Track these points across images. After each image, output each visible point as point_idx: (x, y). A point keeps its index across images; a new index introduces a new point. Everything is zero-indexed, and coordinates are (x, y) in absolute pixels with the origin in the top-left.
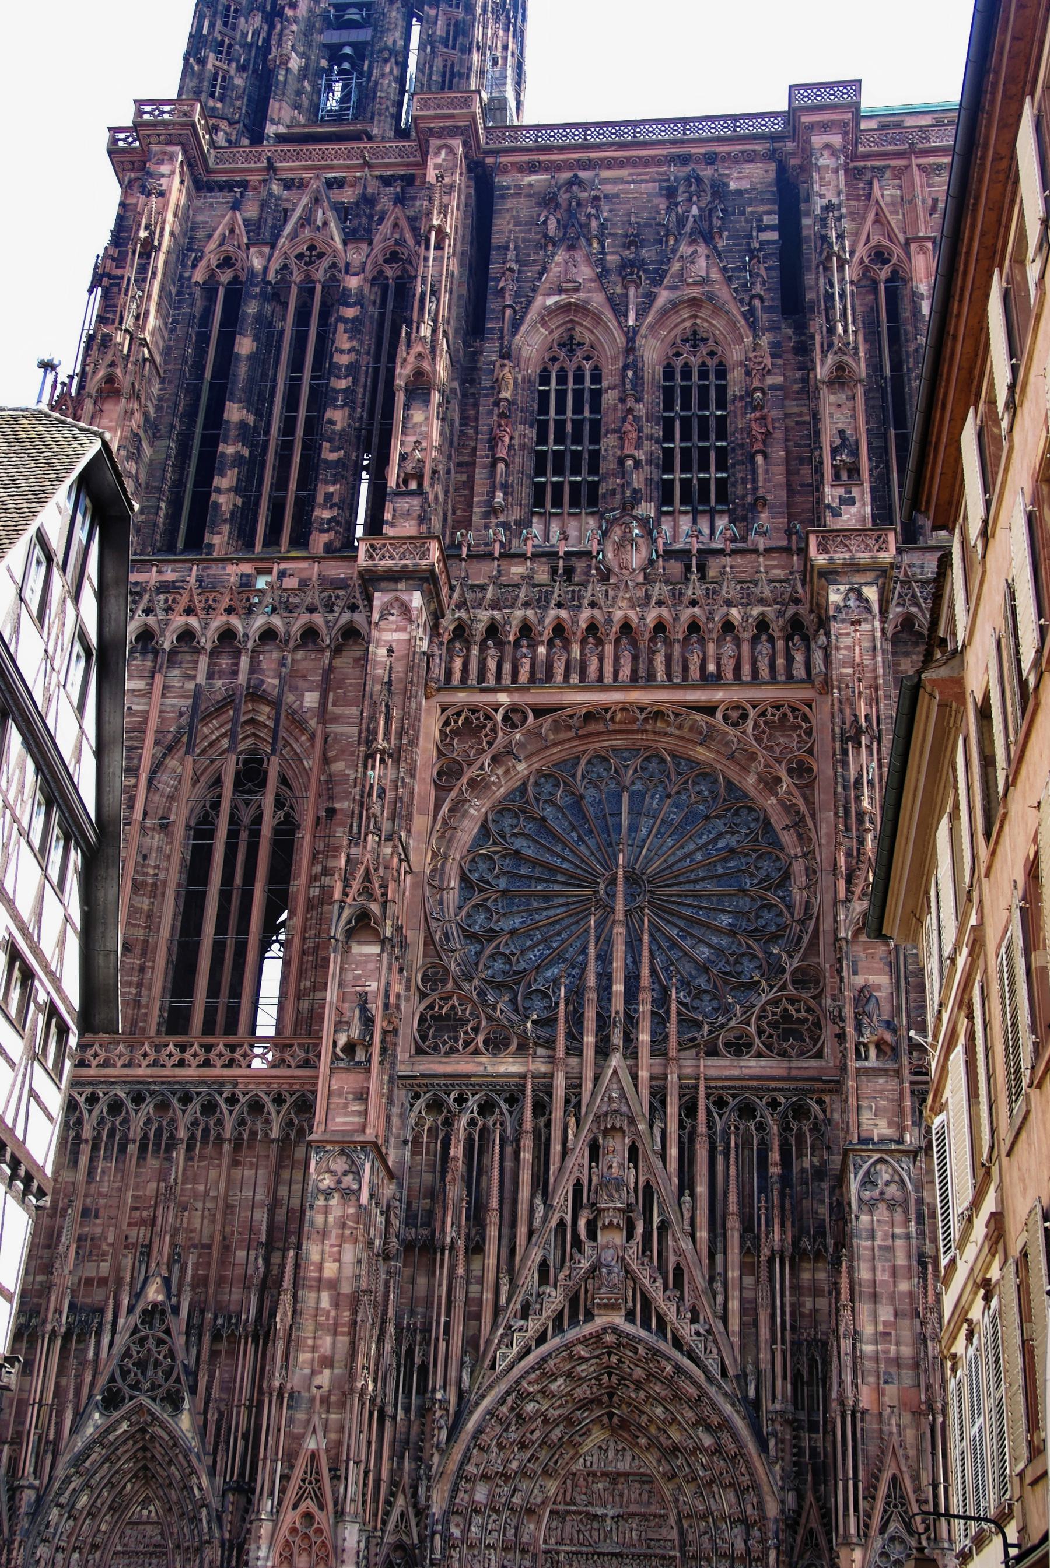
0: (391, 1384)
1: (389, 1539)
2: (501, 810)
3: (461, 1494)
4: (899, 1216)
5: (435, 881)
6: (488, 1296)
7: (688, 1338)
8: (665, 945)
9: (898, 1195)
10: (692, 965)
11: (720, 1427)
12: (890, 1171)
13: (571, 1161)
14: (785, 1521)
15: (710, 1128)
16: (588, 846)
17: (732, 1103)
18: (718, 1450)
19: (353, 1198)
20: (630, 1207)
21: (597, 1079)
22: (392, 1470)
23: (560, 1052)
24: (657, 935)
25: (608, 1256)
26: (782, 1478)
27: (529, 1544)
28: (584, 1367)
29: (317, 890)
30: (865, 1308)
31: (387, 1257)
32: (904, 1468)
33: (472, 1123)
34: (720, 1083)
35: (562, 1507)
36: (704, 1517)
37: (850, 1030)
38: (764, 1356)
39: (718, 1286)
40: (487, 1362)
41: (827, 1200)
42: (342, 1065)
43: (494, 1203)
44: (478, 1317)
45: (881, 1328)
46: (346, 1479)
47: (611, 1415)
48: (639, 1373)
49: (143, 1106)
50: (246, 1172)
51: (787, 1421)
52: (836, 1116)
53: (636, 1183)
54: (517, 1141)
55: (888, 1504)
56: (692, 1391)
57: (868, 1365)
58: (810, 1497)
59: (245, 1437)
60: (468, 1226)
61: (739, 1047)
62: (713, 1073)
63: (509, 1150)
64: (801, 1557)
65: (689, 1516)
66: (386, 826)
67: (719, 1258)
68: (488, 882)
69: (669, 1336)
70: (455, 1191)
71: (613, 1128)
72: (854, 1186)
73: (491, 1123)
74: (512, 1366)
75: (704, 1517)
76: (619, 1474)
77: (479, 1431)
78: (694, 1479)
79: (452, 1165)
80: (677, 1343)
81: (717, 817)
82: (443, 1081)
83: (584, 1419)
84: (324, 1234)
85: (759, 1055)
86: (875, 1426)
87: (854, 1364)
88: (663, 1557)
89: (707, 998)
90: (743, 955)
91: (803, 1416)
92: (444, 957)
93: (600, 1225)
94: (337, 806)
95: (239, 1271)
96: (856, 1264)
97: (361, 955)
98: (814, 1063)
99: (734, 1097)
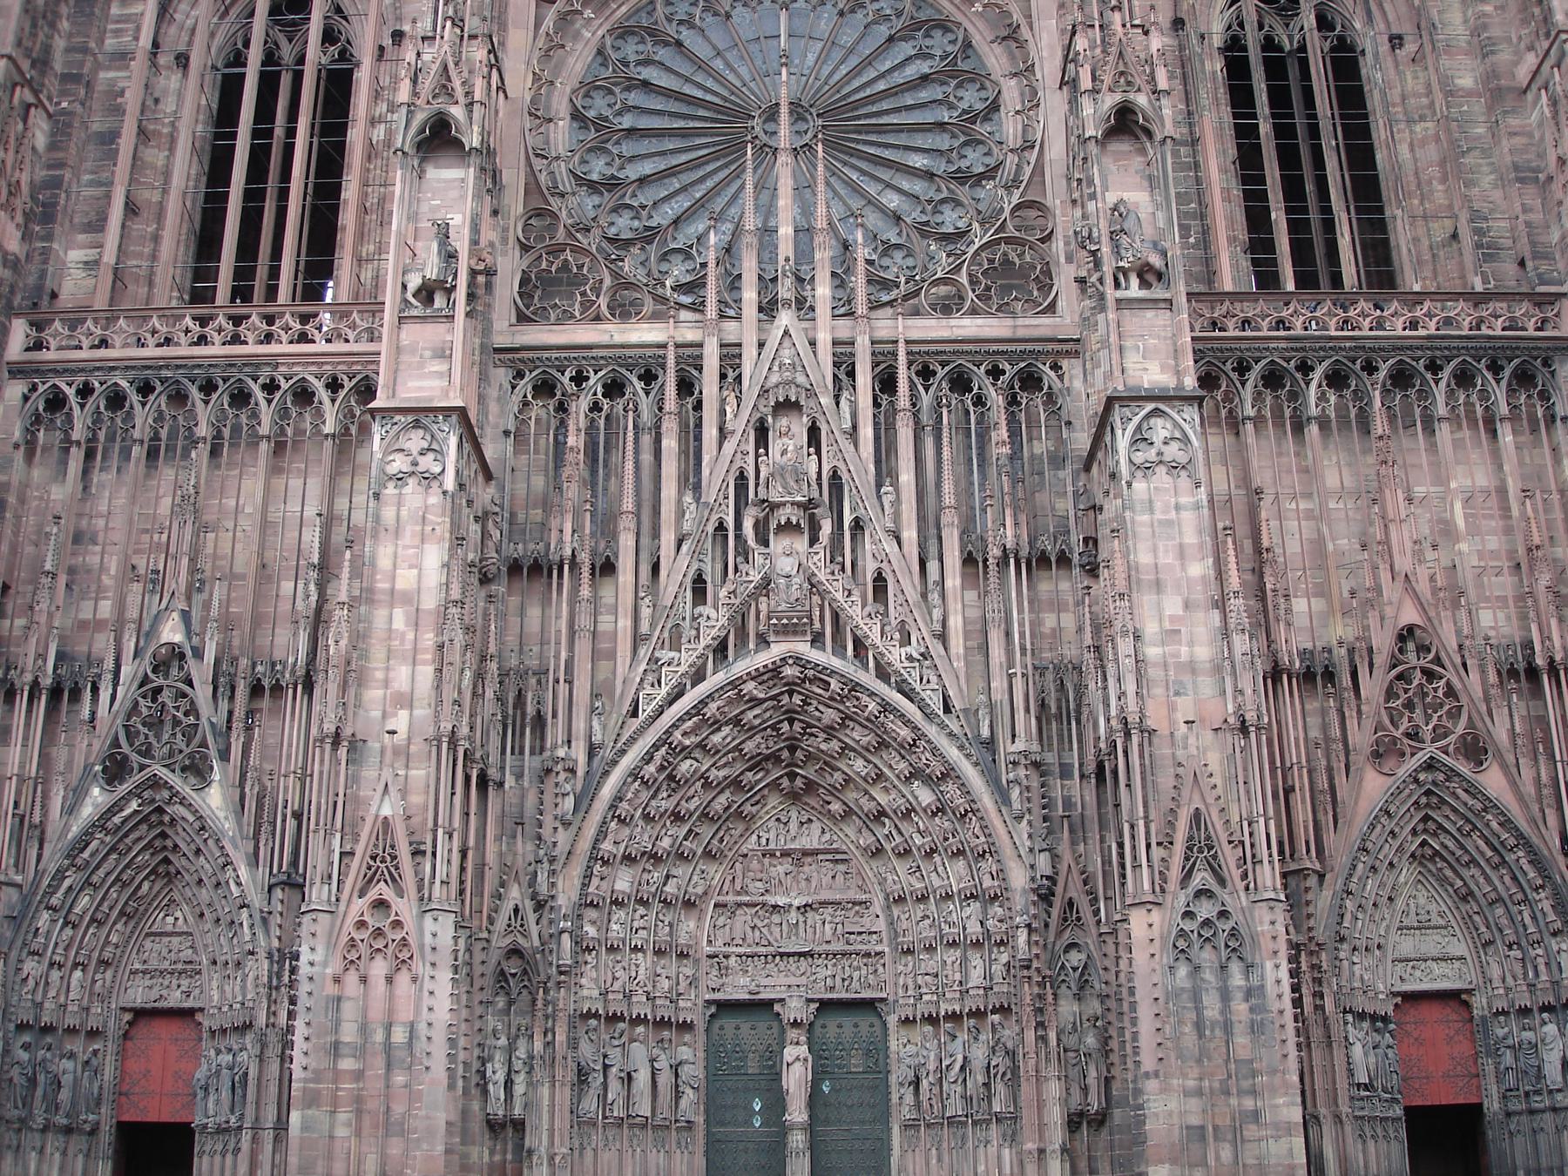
0: (495, 741)
1: (501, 942)
2: (623, 32)
3: (595, 881)
4: (1184, 481)
5: (539, 115)
6: (625, 623)
7: (898, 665)
8: (842, 192)
9: (1182, 458)
10: (878, 215)
11: (944, 777)
12: (1168, 426)
13: (729, 447)
14: (1033, 890)
15: (914, 405)
16: (738, 76)
17: (941, 373)
18: (940, 810)
19: (435, 484)
20: (808, 506)
21: (761, 345)
22: (501, 854)
23: (711, 310)
24: (832, 180)
25: (786, 565)
26: (1030, 836)
27: (689, 946)
28: (757, 711)
29: (382, 133)
30: (1146, 600)
31: (485, 580)
32: (1210, 800)
33: (596, 407)
34: (924, 348)
35: (731, 898)
36: (923, 899)
37: (1106, 249)
38: (998, 684)
39: (934, 597)
40: (626, 707)
41: (1070, 489)
42: (415, 313)
43: (628, 504)
44: (612, 655)
45: (1167, 625)
46: (434, 854)
47: (792, 776)
48: (830, 716)
49: (152, 397)
50: (291, 482)
51: (1036, 765)
52: (1078, 384)
53: (819, 474)
54: (657, 425)
55: (1190, 848)
56: (904, 733)
57: (1154, 673)
58: (1067, 858)
59: (298, 816)
60: (593, 535)
61: (946, 308)
62: (915, 335)
63: (646, 440)
64: (1059, 934)
65: (901, 900)
66: (472, 24)
67: (933, 567)
68: (606, 119)
69: (871, 664)
70: (572, 491)
71: (787, 399)
72: (1123, 442)
73: (621, 407)
74: (660, 712)
75: (923, 899)
76: (806, 853)
77: (619, 798)
78: (908, 852)
79: (570, 457)
80: (883, 673)
81: (904, 39)
82: (555, 355)
83: (760, 780)
84: (397, 533)
85: (974, 312)
86: (1168, 751)
87: (1138, 670)
88: (868, 955)
89: (898, 255)
90: (943, 201)
91: (1051, 758)
92: (551, 199)
93: (773, 525)
94: (406, 28)
95: (285, 607)
96: (1130, 543)
97: (439, 181)
98: (1045, 320)
99: (943, 364)
